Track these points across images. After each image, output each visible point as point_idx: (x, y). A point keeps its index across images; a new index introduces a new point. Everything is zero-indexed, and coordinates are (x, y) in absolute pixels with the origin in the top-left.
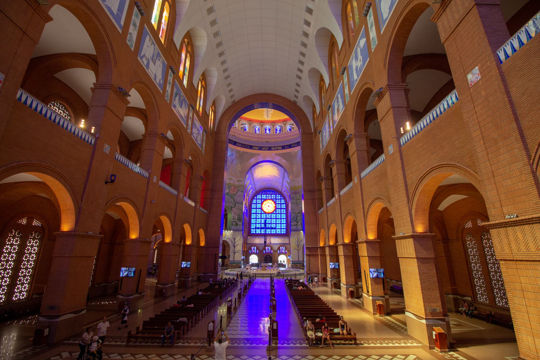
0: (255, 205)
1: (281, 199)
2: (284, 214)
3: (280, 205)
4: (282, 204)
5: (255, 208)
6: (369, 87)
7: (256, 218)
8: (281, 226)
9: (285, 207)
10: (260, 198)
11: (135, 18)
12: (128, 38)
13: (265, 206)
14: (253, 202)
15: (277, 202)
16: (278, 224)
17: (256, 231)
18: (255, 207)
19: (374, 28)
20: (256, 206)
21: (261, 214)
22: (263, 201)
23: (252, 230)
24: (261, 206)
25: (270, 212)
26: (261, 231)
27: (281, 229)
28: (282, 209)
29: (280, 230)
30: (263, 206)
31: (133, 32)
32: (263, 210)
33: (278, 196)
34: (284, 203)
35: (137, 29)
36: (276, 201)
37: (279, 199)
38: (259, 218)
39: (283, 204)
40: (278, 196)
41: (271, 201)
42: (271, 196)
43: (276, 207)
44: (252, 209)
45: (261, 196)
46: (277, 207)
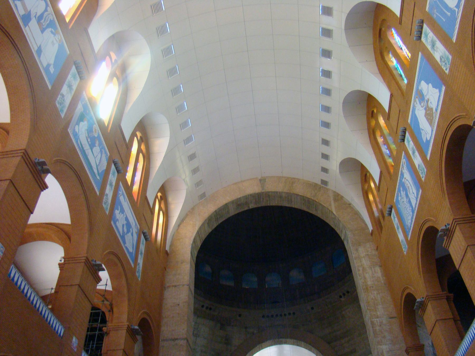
6: (431, 225)
11: (112, 176)
12: (104, 200)
19: (417, 153)
31: (109, 192)
35: (113, 188)
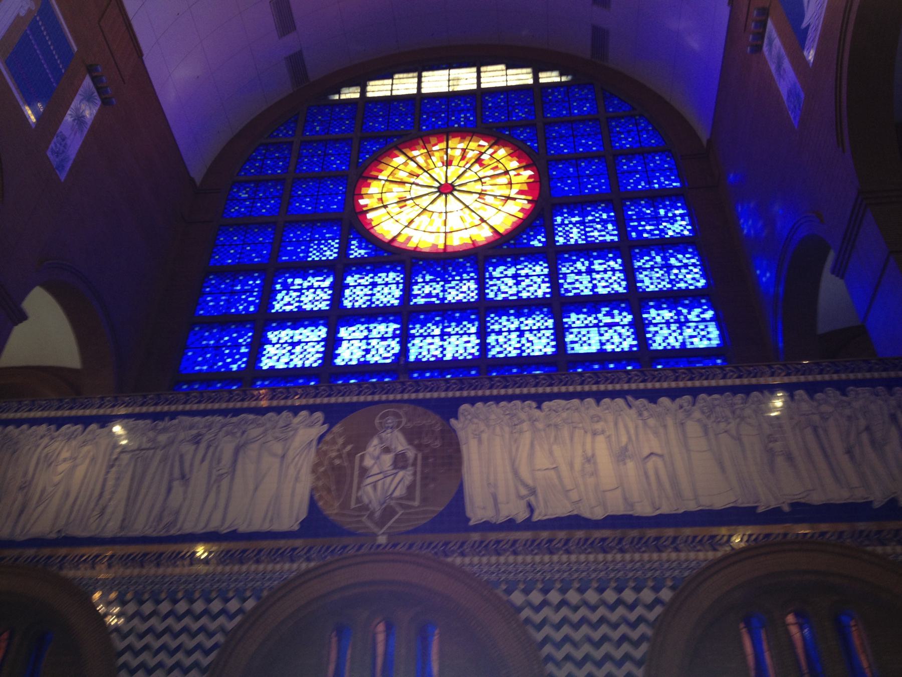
25: (457, 241)
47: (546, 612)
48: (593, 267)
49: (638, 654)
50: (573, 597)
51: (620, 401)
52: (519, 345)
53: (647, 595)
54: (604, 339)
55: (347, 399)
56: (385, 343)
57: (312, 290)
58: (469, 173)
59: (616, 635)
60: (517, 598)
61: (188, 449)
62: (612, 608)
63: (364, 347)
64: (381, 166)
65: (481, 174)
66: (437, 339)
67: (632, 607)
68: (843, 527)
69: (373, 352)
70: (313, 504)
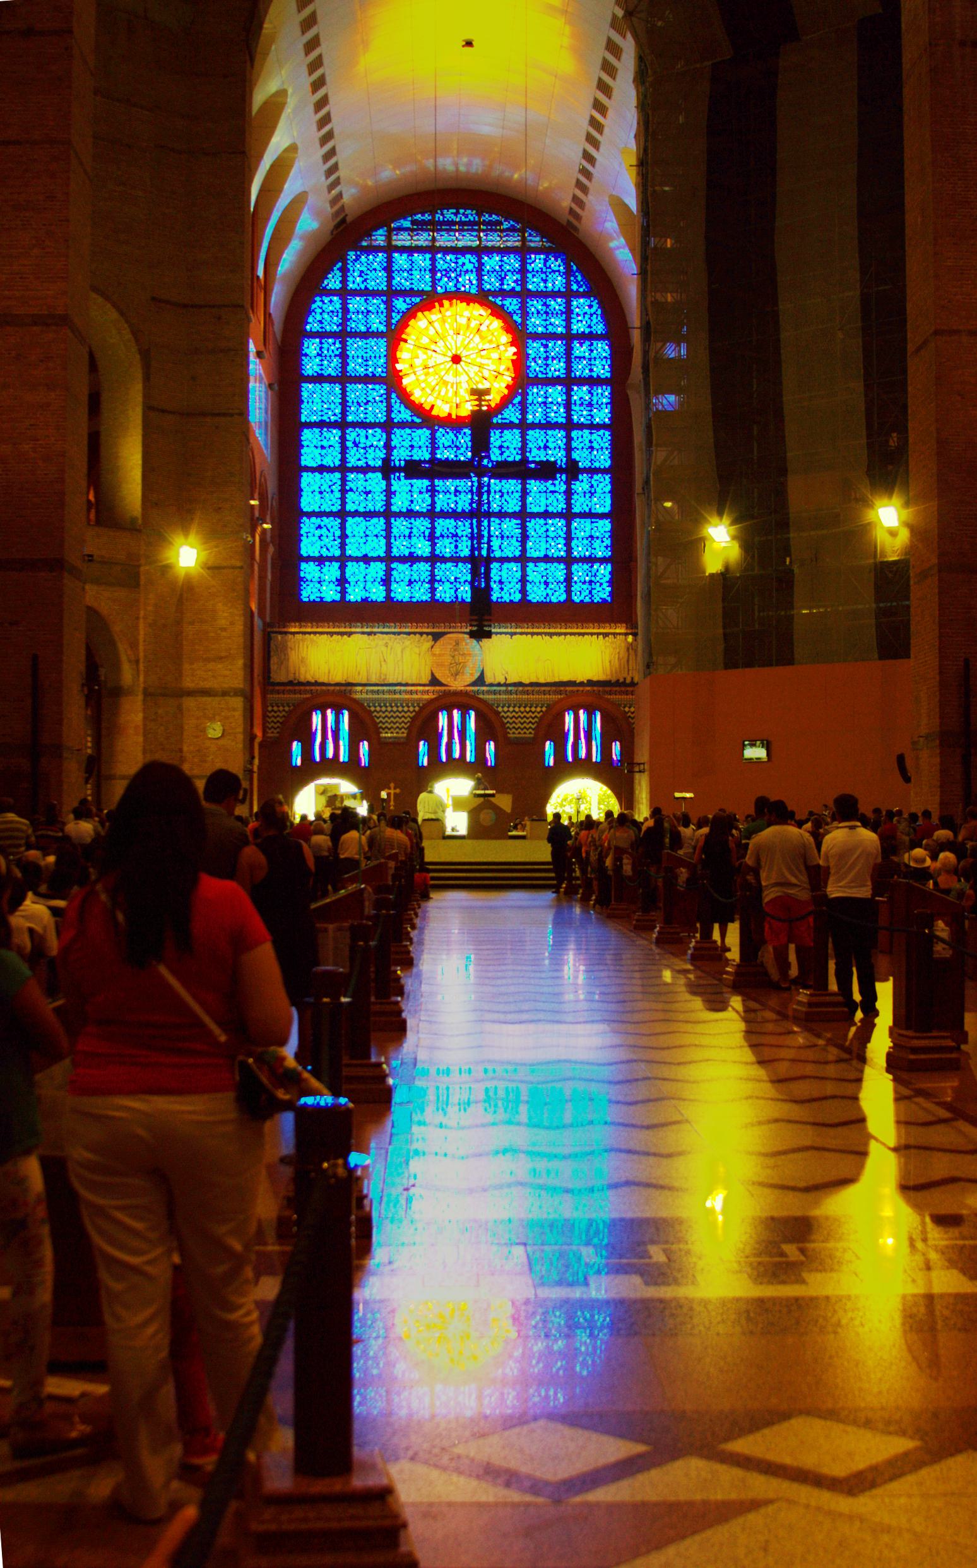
0: (332, 346)
1: (568, 295)
2: (593, 427)
3: (558, 347)
4: (583, 337)
5: (330, 380)
7: (343, 469)
8: (569, 538)
9: (602, 370)
10: (377, 281)
13: (422, 358)
14: (312, 326)
15: (536, 324)
16: (546, 515)
17: (342, 582)
18: (332, 368)
20: (343, 356)
21: (388, 426)
22: (410, 315)
23: (309, 570)
24: (392, 358)
26: (387, 582)
27: (569, 561)
28: (581, 381)
29: (558, 572)
30: (405, 353)
32: (405, 398)
33: (546, 271)
34: (600, 328)
36: (525, 314)
37: (554, 295)
38: (366, 470)
39: (590, 337)
40: (546, 271)
41: (477, 311)
42: (479, 271)
43: (520, 363)
44: (307, 388)
45: (389, 269)
46: (535, 368)
47: (508, 714)
48: (548, 444)
49: (533, 727)
50: (517, 709)
51: (540, 637)
52: (500, 504)
53: (539, 709)
54: (548, 502)
55: (440, 630)
56: (421, 496)
57: (372, 448)
58: (471, 345)
59: (528, 721)
60: (500, 709)
61: (384, 649)
62: (528, 713)
63: (410, 499)
64: (408, 330)
65: (481, 347)
66: (452, 496)
67: (533, 713)
68: (601, 689)
69: (415, 502)
70: (432, 674)
